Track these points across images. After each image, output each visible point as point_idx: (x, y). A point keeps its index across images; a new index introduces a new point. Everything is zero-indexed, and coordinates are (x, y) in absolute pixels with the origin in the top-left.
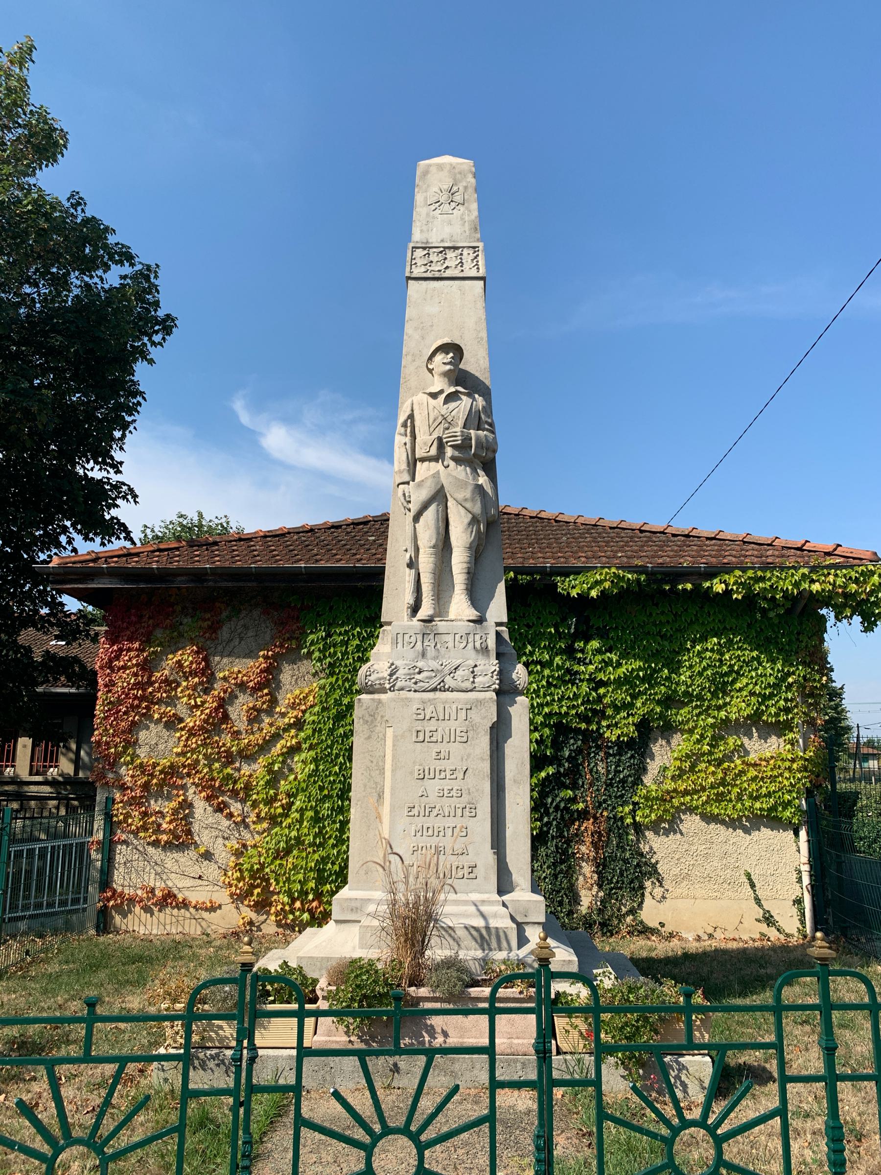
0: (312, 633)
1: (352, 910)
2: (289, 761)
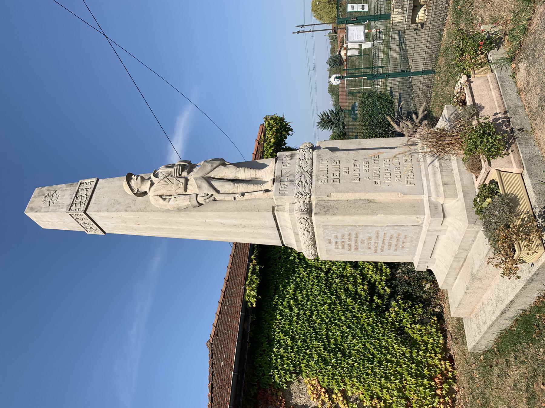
0: (274, 379)
2: (351, 400)
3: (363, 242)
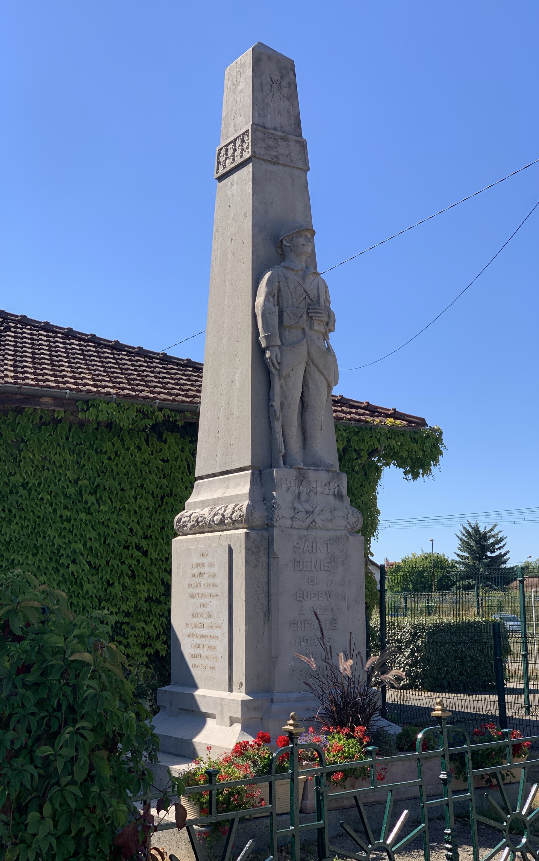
1: (255, 709)
3: (204, 605)
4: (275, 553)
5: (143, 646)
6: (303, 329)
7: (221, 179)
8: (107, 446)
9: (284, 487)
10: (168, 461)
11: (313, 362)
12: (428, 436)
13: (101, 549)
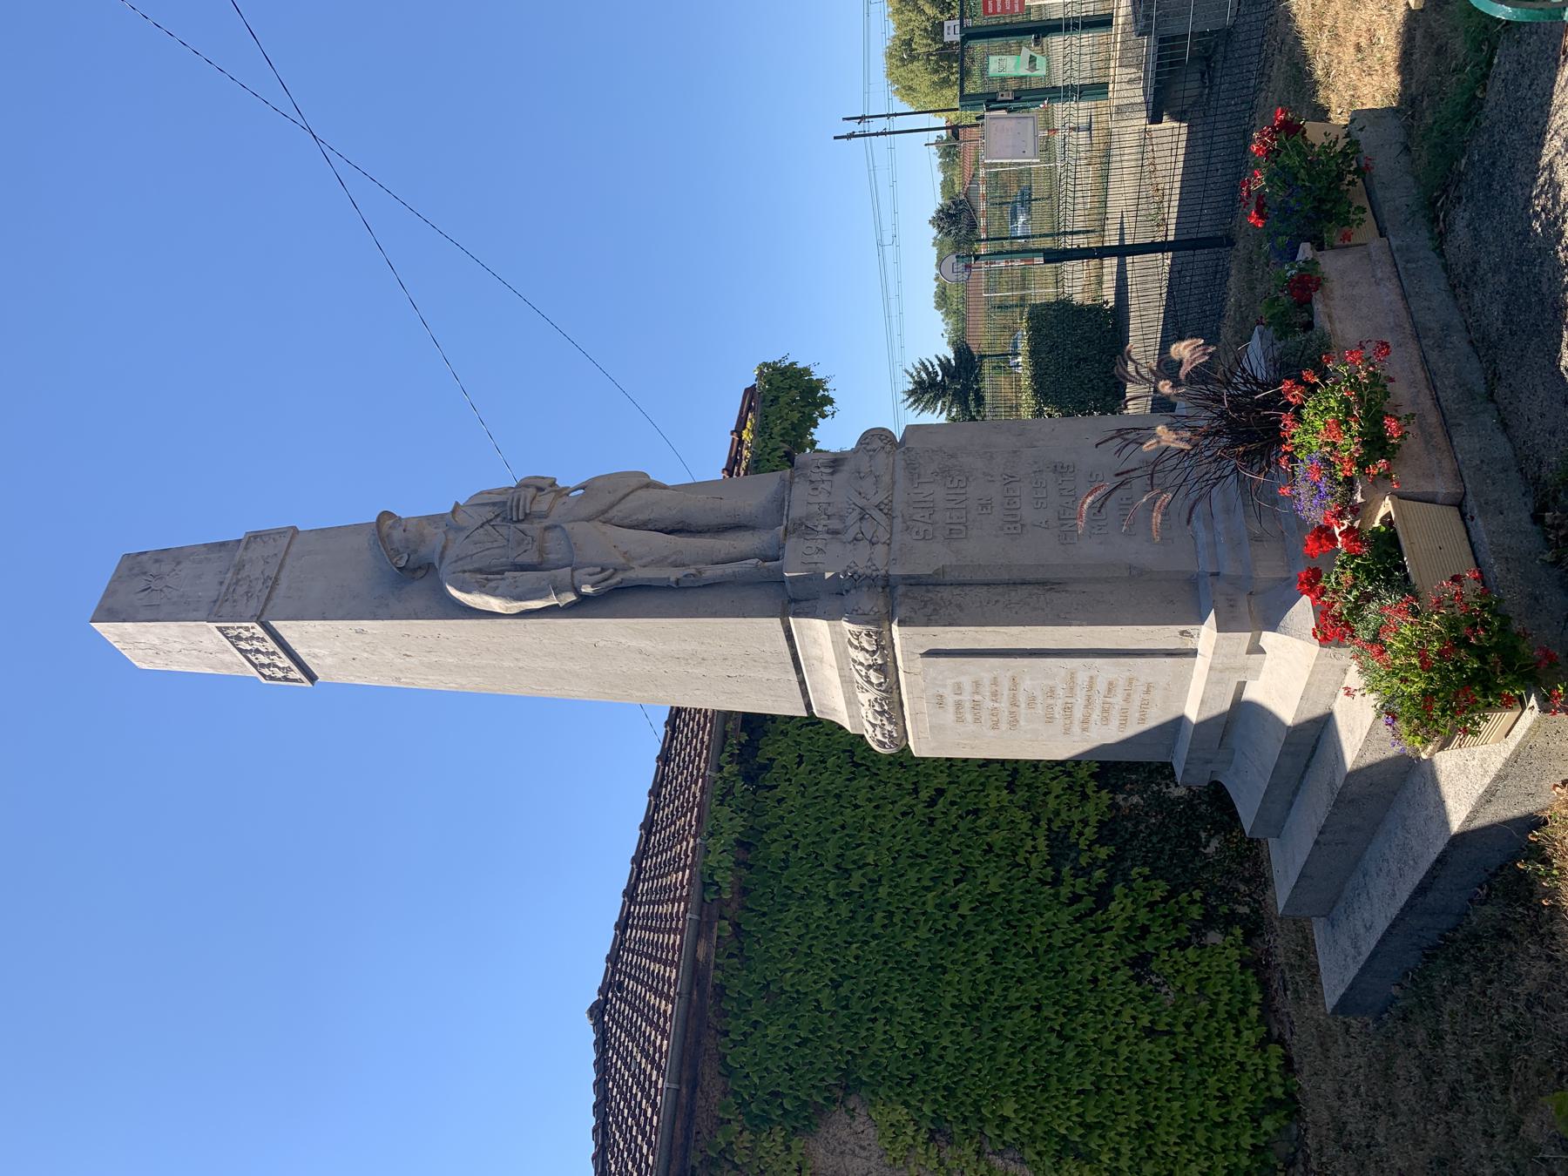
3: (1032, 701)
4: (936, 572)
5: (1084, 797)
6: (547, 528)
7: (312, 678)
8: (776, 851)
9: (816, 558)
10: (800, 756)
11: (604, 512)
12: (770, 382)
13: (935, 863)
